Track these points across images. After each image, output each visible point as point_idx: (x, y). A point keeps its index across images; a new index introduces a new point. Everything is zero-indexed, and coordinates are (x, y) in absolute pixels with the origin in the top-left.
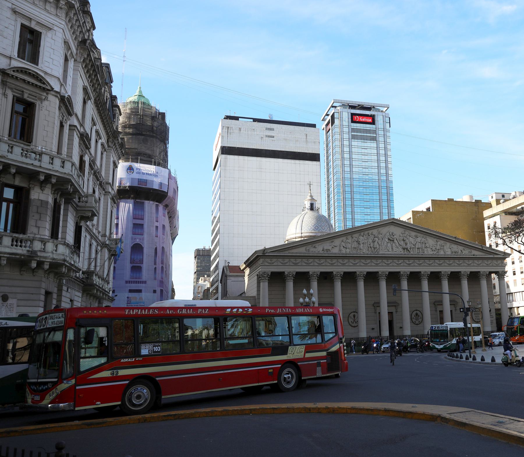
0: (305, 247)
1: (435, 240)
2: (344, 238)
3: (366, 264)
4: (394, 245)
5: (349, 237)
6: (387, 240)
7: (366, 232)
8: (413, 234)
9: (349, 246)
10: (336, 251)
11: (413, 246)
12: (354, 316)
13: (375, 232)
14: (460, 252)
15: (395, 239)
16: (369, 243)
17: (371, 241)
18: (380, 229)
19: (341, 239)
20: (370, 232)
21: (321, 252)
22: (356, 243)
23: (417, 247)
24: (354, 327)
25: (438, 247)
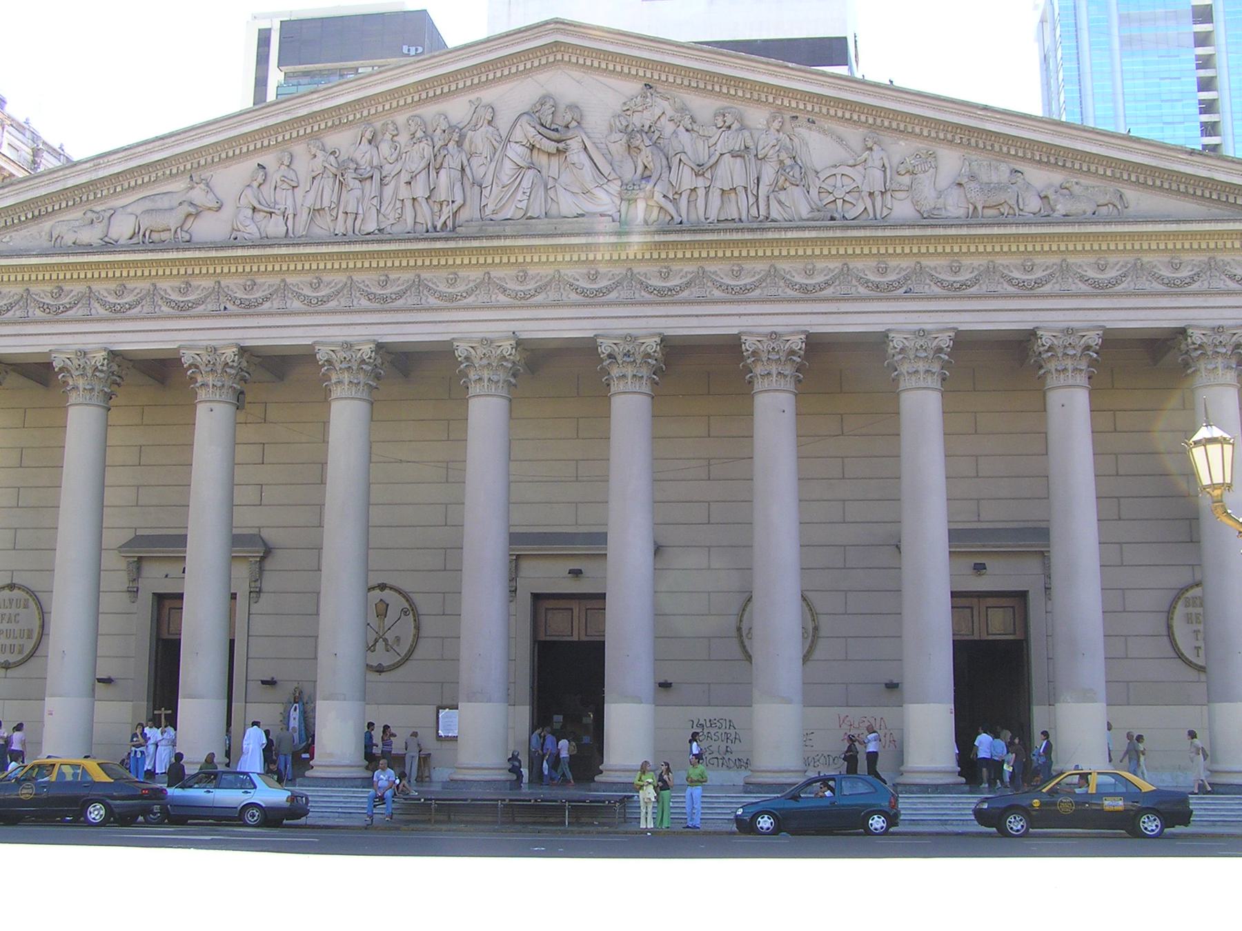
0: (47, 225)
1: (854, 136)
2: (268, 159)
3: (384, 299)
4: (565, 178)
5: (299, 149)
6: (516, 152)
7: (401, 119)
8: (703, 106)
9: (285, 199)
10: (209, 228)
11: (687, 180)
12: (382, 610)
13: (458, 109)
14: (1033, 204)
15: (574, 144)
16: (405, 177)
17: (416, 164)
18: (488, 95)
19: (244, 169)
20: (429, 111)
21: (121, 242)
22: (328, 184)
23: (718, 184)
24: (380, 670)
25: (875, 179)
